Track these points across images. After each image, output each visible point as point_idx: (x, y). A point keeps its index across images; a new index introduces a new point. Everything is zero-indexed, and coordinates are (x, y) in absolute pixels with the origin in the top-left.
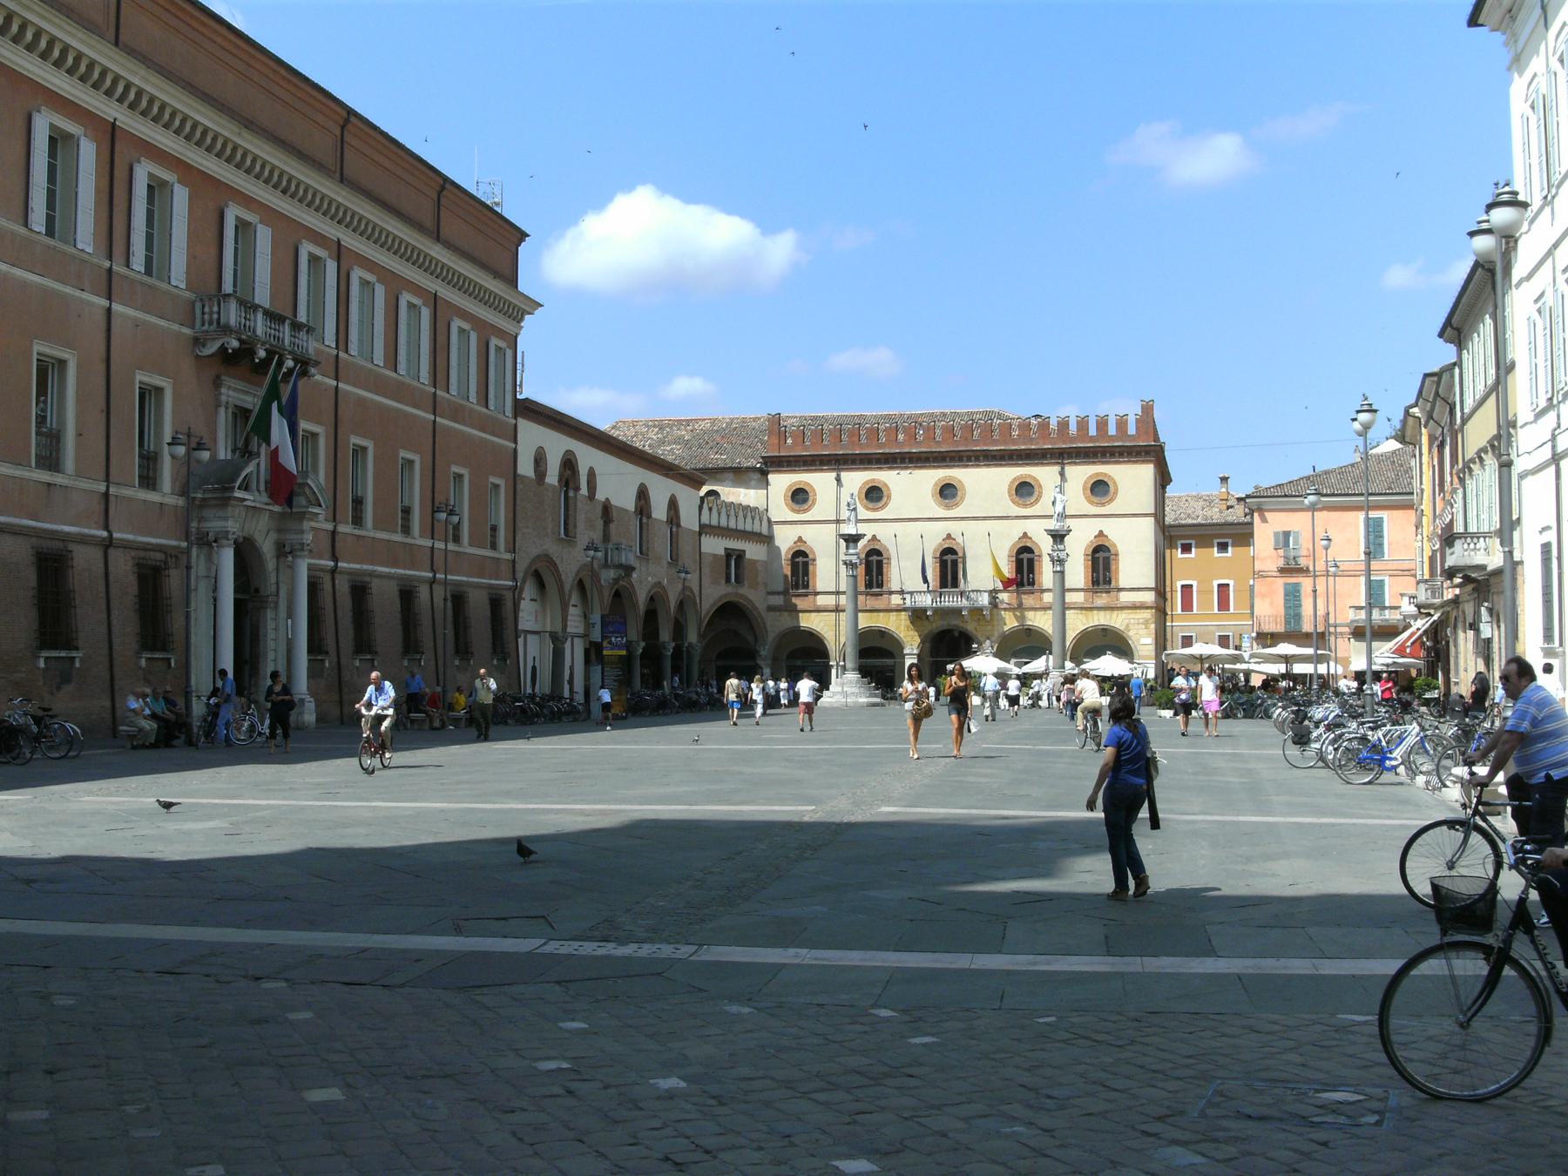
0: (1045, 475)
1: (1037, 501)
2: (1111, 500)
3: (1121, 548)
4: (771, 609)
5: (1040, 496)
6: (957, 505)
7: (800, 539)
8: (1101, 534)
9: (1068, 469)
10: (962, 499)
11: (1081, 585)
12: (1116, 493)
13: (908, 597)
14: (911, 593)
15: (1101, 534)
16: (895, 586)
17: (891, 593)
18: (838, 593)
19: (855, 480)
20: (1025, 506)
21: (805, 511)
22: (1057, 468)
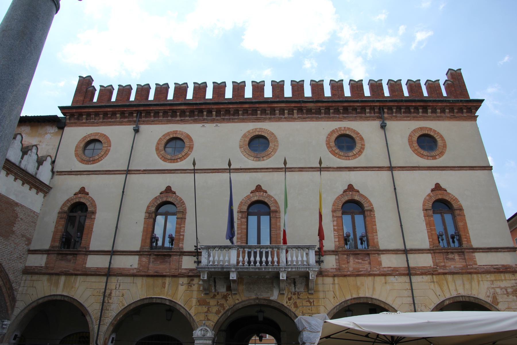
0: (366, 128)
1: (360, 152)
2: (442, 153)
3: (464, 203)
4: (28, 271)
5: (362, 148)
6: (269, 156)
7: (83, 191)
8: (438, 187)
9: (391, 124)
10: (275, 150)
11: (426, 245)
12: (445, 146)
13: (204, 254)
14: (208, 248)
15: (438, 187)
16: (188, 246)
17: (183, 253)
18: (113, 253)
19: (155, 132)
20: (348, 158)
21: (94, 161)
22: (377, 123)
